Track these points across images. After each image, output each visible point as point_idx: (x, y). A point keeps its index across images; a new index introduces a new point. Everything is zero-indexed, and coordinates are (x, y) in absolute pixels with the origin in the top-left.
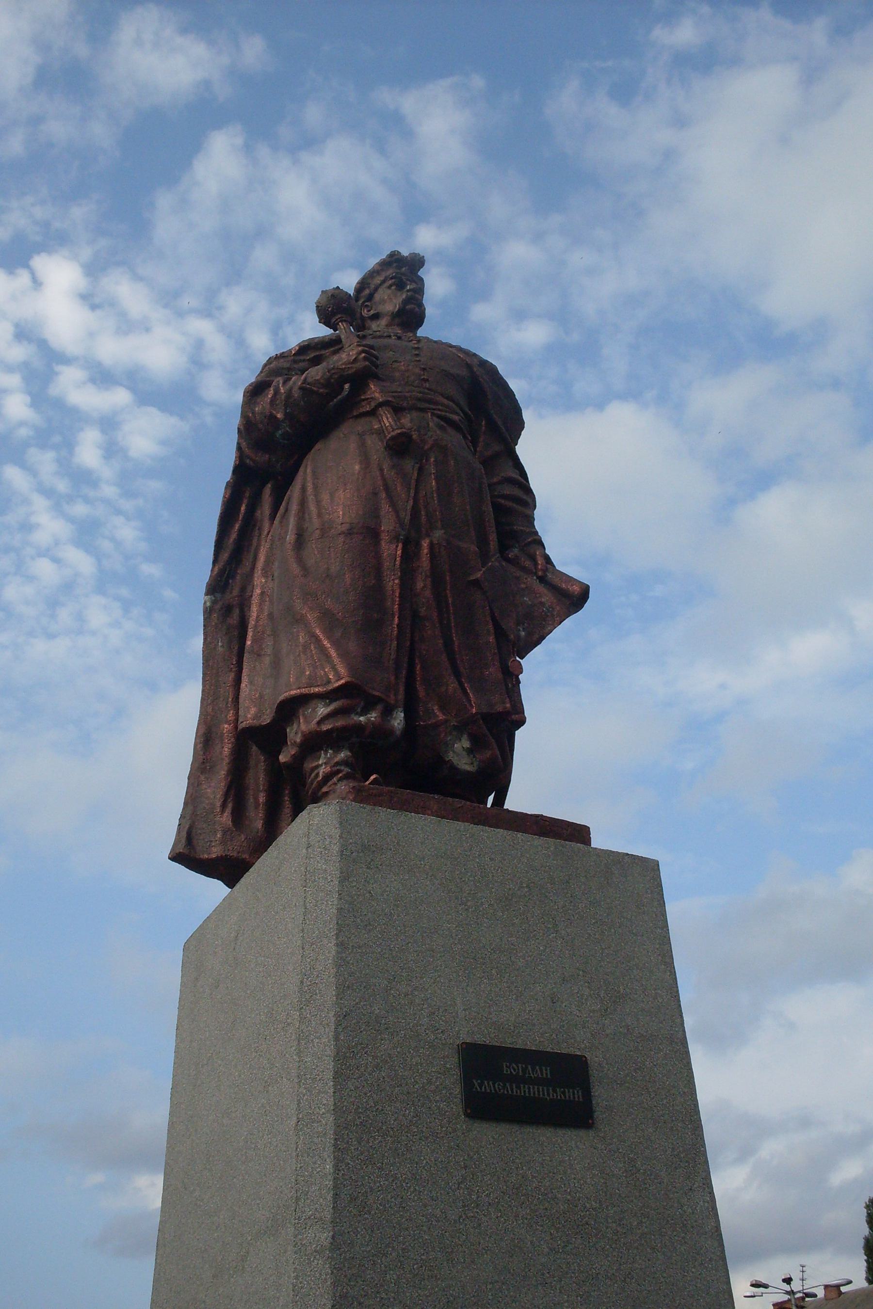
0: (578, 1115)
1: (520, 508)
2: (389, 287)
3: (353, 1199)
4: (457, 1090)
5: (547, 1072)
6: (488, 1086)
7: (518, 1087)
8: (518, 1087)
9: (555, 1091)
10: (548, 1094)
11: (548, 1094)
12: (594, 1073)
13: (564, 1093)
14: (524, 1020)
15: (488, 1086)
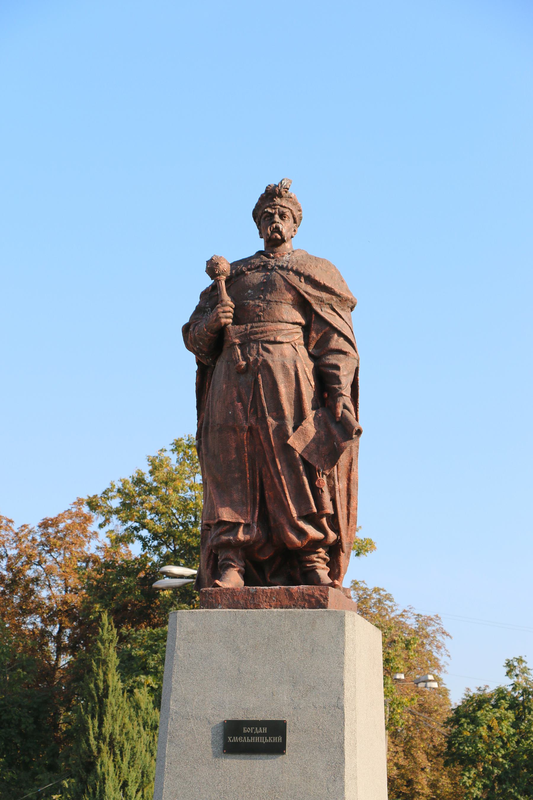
0: (279, 749)
1: (335, 371)
2: (265, 218)
3: (171, 793)
4: (221, 742)
5: (265, 730)
6: (236, 739)
7: (250, 738)
8: (250, 738)
9: (268, 738)
10: (264, 741)
11: (264, 741)
12: (289, 728)
13: (272, 739)
14: (255, 707)
15: (236, 739)
